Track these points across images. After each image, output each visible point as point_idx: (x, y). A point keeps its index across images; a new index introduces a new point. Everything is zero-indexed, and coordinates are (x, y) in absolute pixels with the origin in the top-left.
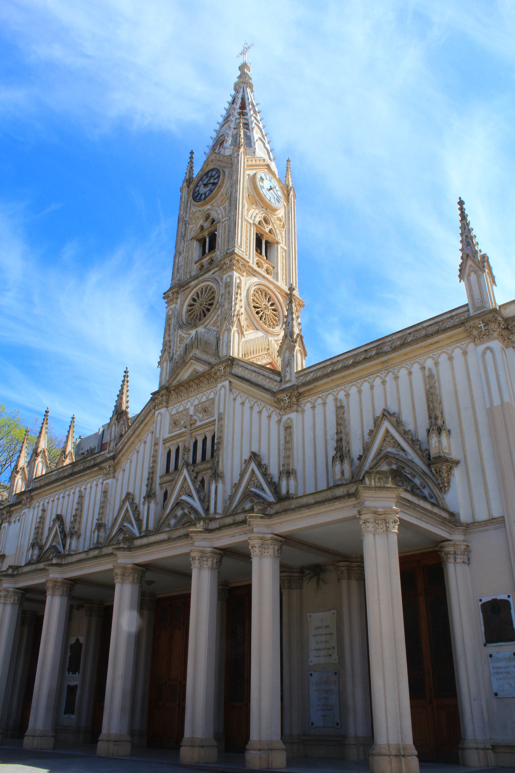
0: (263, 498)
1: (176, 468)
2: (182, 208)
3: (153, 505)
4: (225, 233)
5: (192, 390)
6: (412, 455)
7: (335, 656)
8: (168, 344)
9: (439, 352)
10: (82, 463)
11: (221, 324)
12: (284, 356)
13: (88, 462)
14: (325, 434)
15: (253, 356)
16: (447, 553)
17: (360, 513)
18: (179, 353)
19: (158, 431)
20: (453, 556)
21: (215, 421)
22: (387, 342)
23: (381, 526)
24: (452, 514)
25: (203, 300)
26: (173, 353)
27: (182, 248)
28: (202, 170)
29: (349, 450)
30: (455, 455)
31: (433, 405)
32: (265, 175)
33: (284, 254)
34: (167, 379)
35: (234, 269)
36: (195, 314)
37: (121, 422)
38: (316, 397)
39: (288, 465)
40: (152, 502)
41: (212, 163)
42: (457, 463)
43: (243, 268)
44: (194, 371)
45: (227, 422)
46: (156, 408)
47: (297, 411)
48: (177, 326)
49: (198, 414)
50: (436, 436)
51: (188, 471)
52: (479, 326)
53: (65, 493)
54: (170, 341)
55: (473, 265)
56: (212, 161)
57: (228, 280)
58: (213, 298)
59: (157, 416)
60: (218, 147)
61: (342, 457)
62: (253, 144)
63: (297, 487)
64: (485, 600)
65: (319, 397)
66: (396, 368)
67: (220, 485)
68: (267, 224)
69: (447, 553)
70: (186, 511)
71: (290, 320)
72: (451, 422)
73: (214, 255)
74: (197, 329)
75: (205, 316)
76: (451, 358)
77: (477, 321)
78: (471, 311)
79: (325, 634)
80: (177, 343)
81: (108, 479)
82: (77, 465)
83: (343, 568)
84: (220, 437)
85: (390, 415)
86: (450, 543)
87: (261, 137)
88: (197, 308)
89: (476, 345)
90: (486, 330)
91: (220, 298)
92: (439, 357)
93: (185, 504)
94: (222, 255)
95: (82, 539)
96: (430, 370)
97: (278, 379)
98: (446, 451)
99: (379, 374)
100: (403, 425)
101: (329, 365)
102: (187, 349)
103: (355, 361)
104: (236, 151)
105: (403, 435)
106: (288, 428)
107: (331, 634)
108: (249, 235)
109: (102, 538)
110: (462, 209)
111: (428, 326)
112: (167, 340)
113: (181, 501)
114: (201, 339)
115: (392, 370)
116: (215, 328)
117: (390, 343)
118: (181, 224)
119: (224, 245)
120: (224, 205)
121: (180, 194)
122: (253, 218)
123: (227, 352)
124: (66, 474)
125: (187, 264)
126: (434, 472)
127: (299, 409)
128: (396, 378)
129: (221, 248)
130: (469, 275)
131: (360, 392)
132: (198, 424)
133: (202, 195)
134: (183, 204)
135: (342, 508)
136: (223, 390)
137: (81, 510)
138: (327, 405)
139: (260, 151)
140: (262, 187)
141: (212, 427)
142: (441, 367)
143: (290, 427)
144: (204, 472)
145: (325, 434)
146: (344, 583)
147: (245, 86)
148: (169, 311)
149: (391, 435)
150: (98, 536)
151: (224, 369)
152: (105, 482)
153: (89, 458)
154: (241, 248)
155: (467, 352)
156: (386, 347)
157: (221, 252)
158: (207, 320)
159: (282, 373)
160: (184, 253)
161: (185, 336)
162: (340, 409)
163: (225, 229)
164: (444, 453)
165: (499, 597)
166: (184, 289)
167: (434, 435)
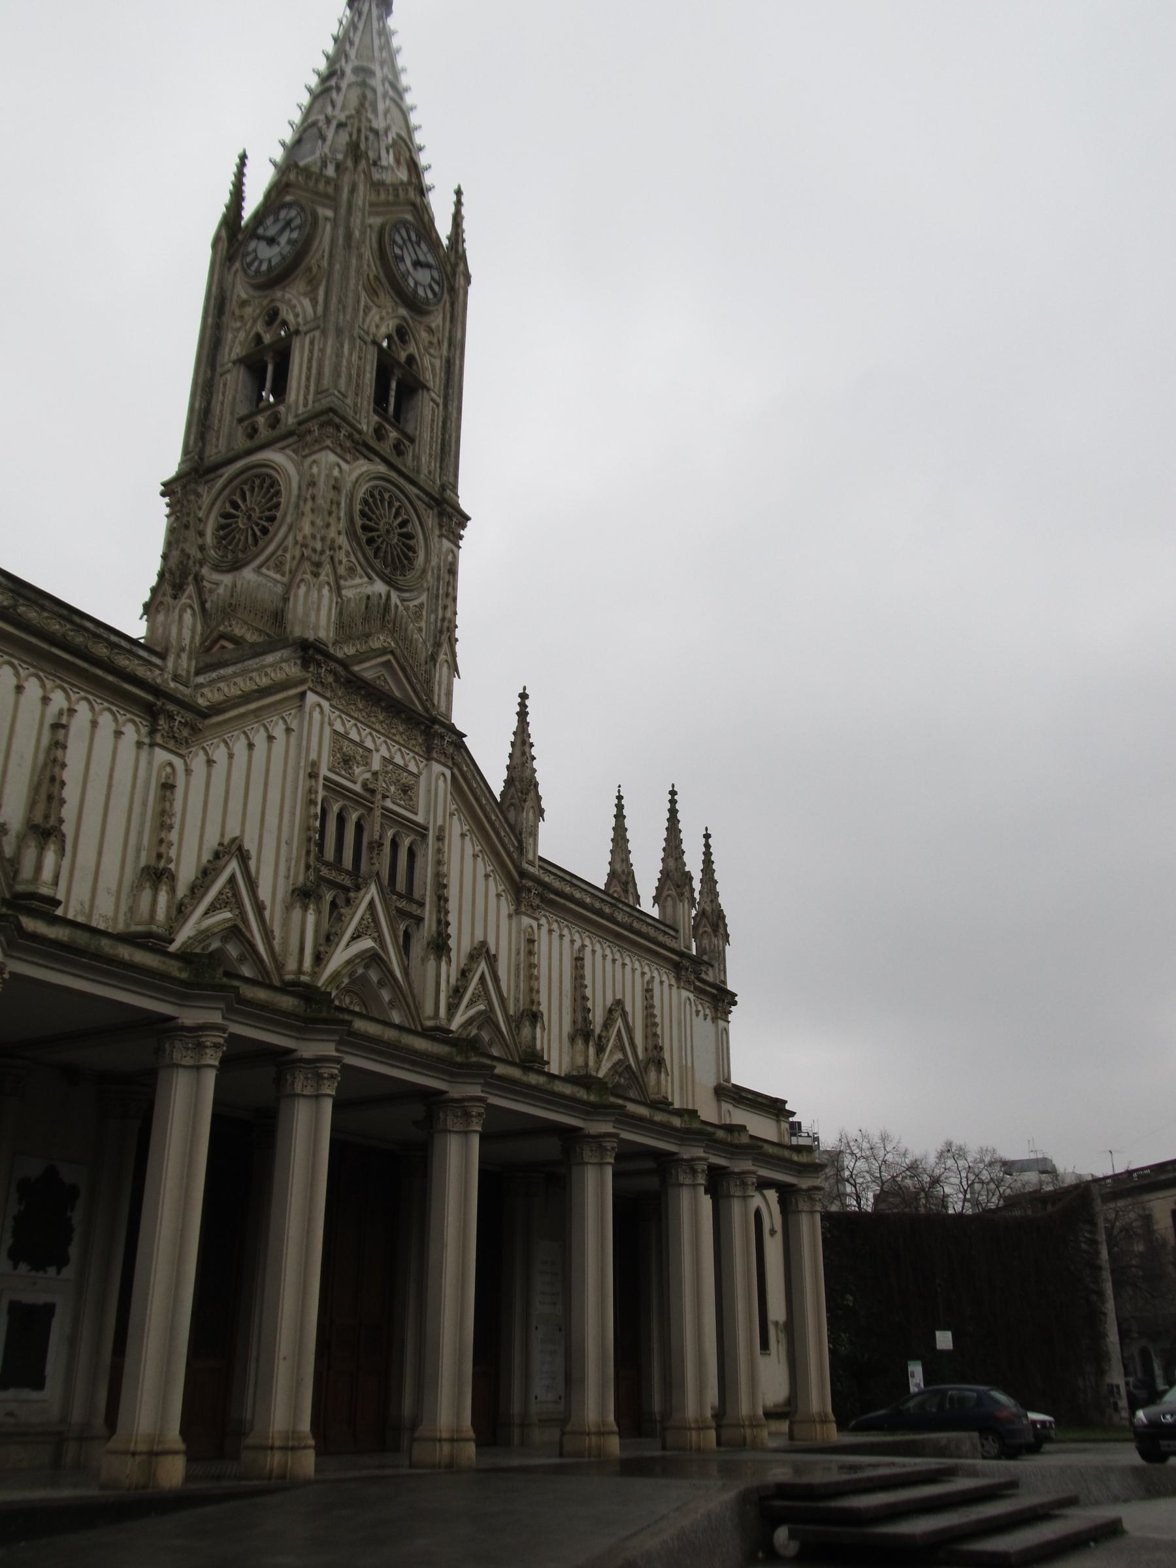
10: (61, 616)
82: (43, 608)
97: (516, 844)
162: (578, 960)
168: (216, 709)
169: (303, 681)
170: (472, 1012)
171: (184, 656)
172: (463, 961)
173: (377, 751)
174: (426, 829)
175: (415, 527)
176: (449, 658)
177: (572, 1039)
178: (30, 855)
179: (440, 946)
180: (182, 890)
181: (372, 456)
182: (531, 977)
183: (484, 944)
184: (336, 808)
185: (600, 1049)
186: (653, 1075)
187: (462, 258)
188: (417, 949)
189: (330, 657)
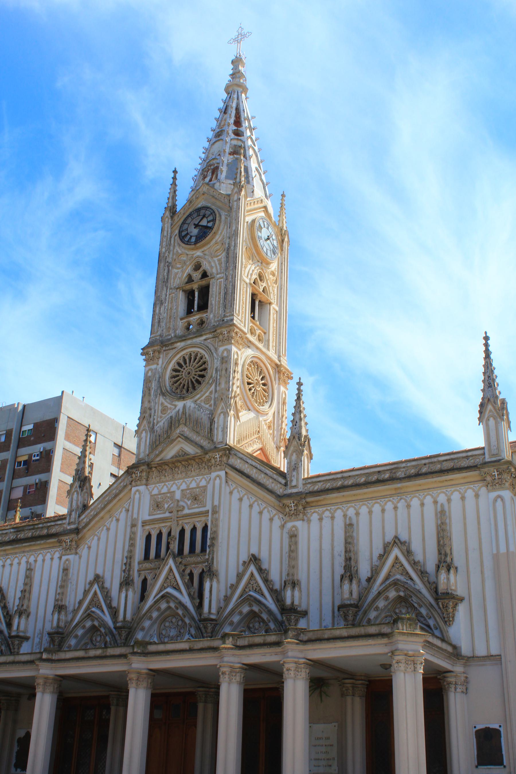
0: (264, 605)
1: (158, 555)
2: (164, 244)
3: (130, 593)
4: (220, 293)
5: (179, 472)
6: (419, 585)
7: (335, 767)
8: (148, 411)
9: (453, 489)
10: (30, 529)
11: (215, 403)
12: (290, 459)
13: (39, 530)
14: (333, 549)
15: (246, 442)
16: (449, 683)
17: (393, 652)
18: (161, 424)
19: (136, 511)
20: (454, 686)
21: (208, 512)
22: (401, 468)
23: (410, 666)
24: (455, 647)
25: (192, 368)
26: (154, 423)
27: (164, 296)
28: (190, 202)
29: (357, 570)
30: (460, 592)
31: (444, 542)
32: (264, 222)
33: (275, 316)
34: (147, 452)
35: (232, 343)
36: (181, 383)
37: (85, 491)
38: (325, 509)
39: (293, 575)
40: (130, 590)
41: (203, 197)
42: (462, 599)
43: (240, 342)
44: (180, 451)
45: (222, 516)
46: (133, 483)
47: (303, 520)
48: (159, 391)
49: (186, 500)
50: (445, 573)
51: (175, 562)
52: (493, 474)
53: (5, 561)
54: (150, 409)
55: (493, 410)
56: (203, 194)
57: (225, 354)
58: (205, 369)
59: (135, 494)
60: (210, 173)
61: (351, 577)
62: (250, 179)
63: (300, 598)
64: (479, 727)
65: (327, 510)
66: (408, 496)
67: (215, 584)
68: (261, 280)
69: (449, 683)
70: (172, 605)
71: (297, 419)
72: (458, 559)
73: (205, 315)
74: (185, 402)
75: (194, 388)
76: (463, 498)
77: (492, 469)
78: (487, 456)
79: (325, 745)
80: (158, 412)
81: (68, 555)
82: (23, 530)
83: (348, 685)
84: (215, 532)
85: (401, 543)
86: (452, 674)
87: (257, 166)
88: (183, 375)
89: (489, 491)
90: (499, 479)
91: (214, 372)
92: (452, 494)
93: (173, 598)
94: (216, 319)
95: (32, 618)
96: (442, 505)
97: (283, 481)
98: (453, 588)
99: (391, 499)
100: (412, 555)
101: (340, 478)
102: (173, 423)
103: (367, 480)
104: (236, 192)
105: (413, 565)
106: (293, 536)
107: (331, 745)
108: (245, 299)
109: (62, 622)
110: (486, 345)
111: (444, 461)
112: (146, 406)
113: (168, 595)
114: (190, 416)
115: (404, 497)
116: (207, 406)
117: (404, 470)
118: (162, 264)
119: (219, 308)
120: (220, 257)
121: (161, 224)
122: (249, 277)
123: (223, 438)
124: (7, 539)
125: (170, 317)
126: (441, 606)
127: (305, 518)
128: (409, 506)
129: (215, 311)
130: (488, 420)
131: (370, 512)
132: (186, 511)
133: (191, 237)
134: (165, 240)
135: (375, 645)
136: (218, 481)
137: (31, 586)
138: (335, 520)
139: (259, 192)
140: (260, 238)
141: (203, 519)
142: (453, 504)
143: (296, 536)
144: (194, 566)
145: (333, 549)
146: (349, 699)
147: (240, 90)
148: (148, 372)
149: (400, 563)
150: (59, 619)
151: (221, 457)
152: (64, 558)
153: (40, 526)
154: (239, 316)
155: (479, 496)
156: (400, 473)
157: (214, 316)
158: (198, 394)
159: (287, 476)
160: (167, 302)
161: (169, 406)
163: (220, 288)
164: (451, 590)
165: (492, 726)
166: (167, 348)
167: (443, 571)
181: (176, 345)
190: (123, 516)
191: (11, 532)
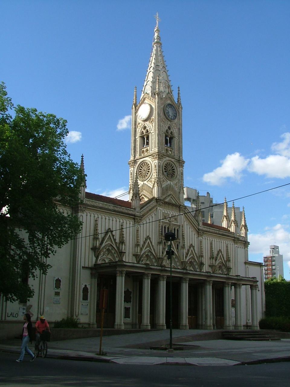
162: (211, 244)
168: (143, 216)
169: (156, 206)
170: (190, 257)
171: (138, 208)
172: (188, 248)
173: (170, 213)
174: (180, 226)
175: (175, 168)
176: (183, 192)
177: (210, 258)
178: (121, 246)
179: (183, 247)
180: (141, 246)
182: (201, 249)
183: (192, 244)
184: (164, 226)
185: (216, 260)
186: (228, 263)
187: (180, 104)
188: (179, 248)
189: (160, 200)
190: (153, 216)
191: (112, 206)
